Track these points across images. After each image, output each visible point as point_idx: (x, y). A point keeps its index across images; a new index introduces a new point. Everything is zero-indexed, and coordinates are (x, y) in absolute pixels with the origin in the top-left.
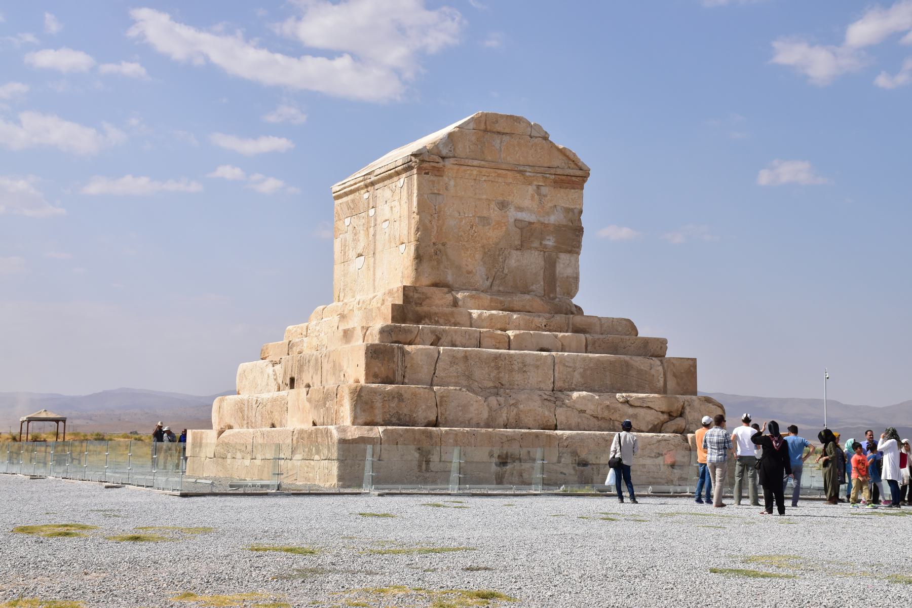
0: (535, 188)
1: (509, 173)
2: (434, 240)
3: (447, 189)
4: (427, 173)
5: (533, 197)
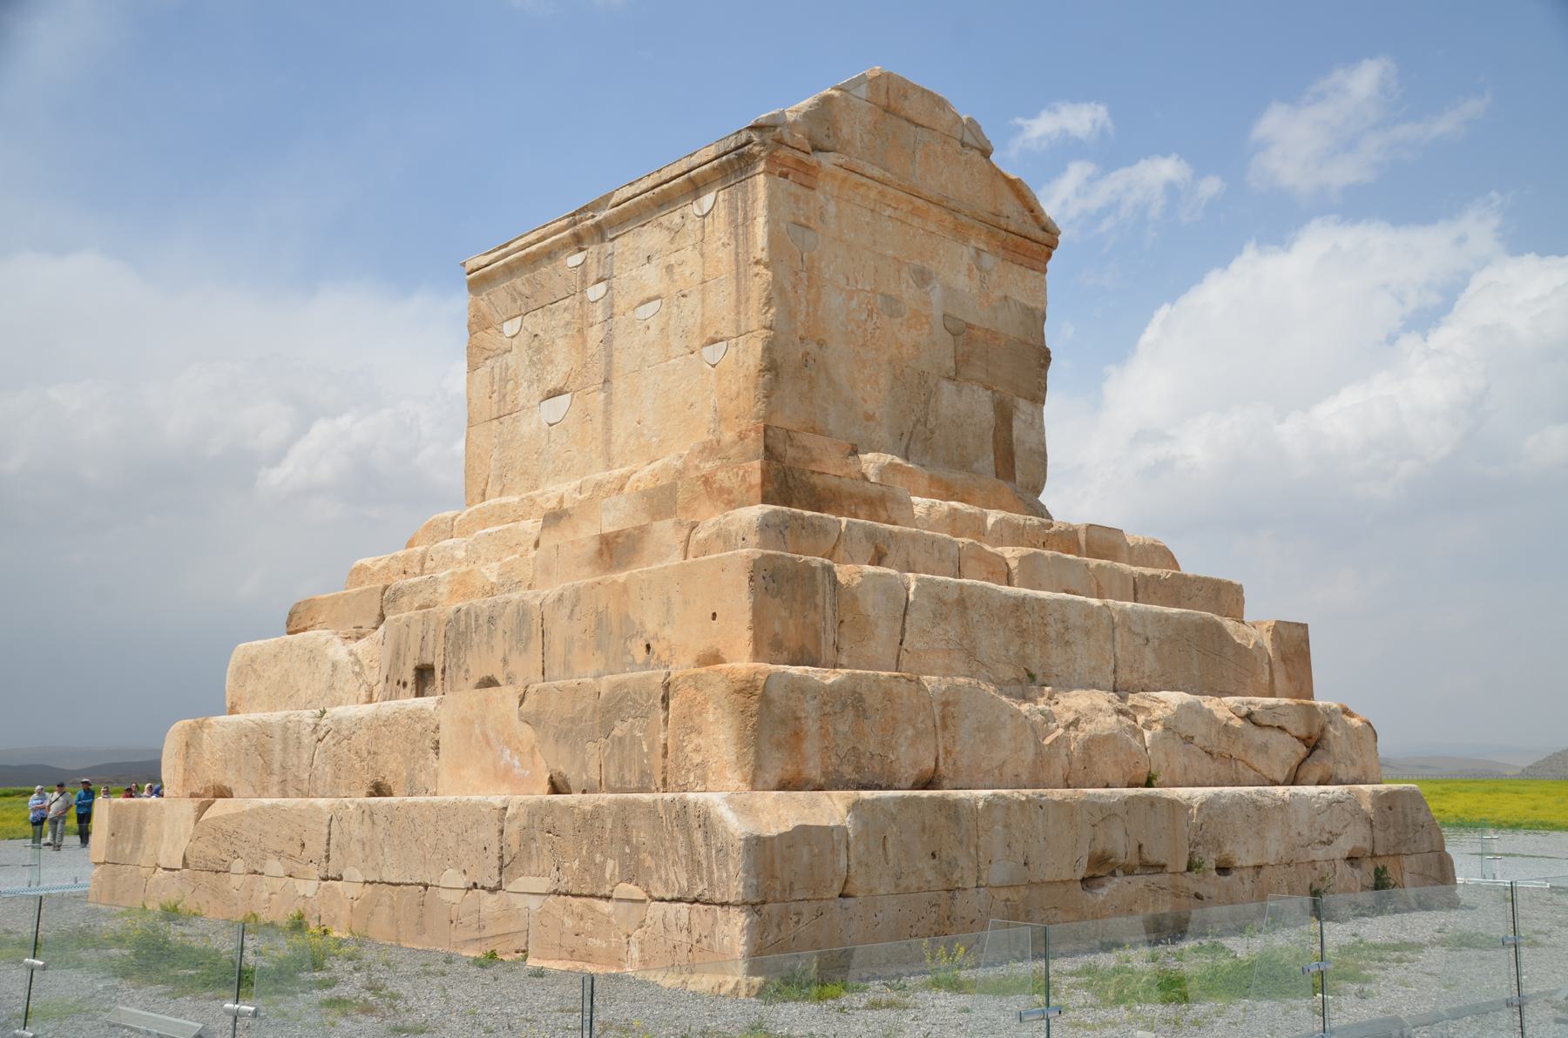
0: (973, 252)
1: (935, 210)
2: (801, 332)
3: (822, 218)
4: (785, 175)
5: (970, 270)
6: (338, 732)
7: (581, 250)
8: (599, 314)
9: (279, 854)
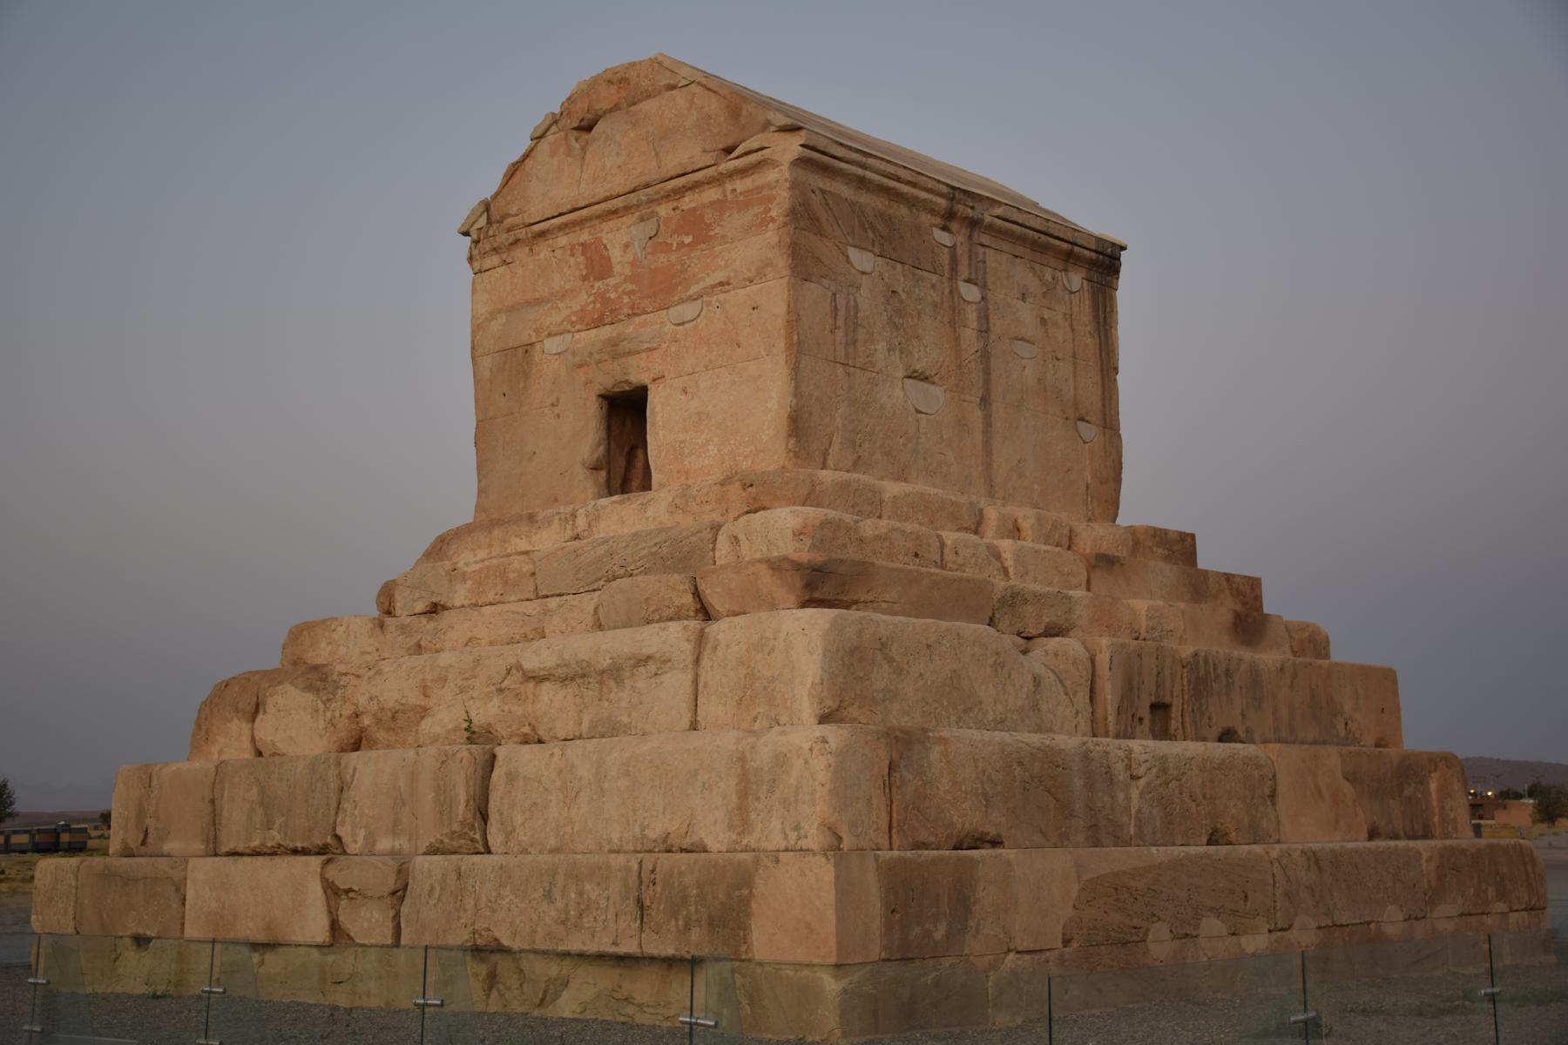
6: (1164, 770)
7: (945, 228)
8: (972, 315)
9: (1216, 911)
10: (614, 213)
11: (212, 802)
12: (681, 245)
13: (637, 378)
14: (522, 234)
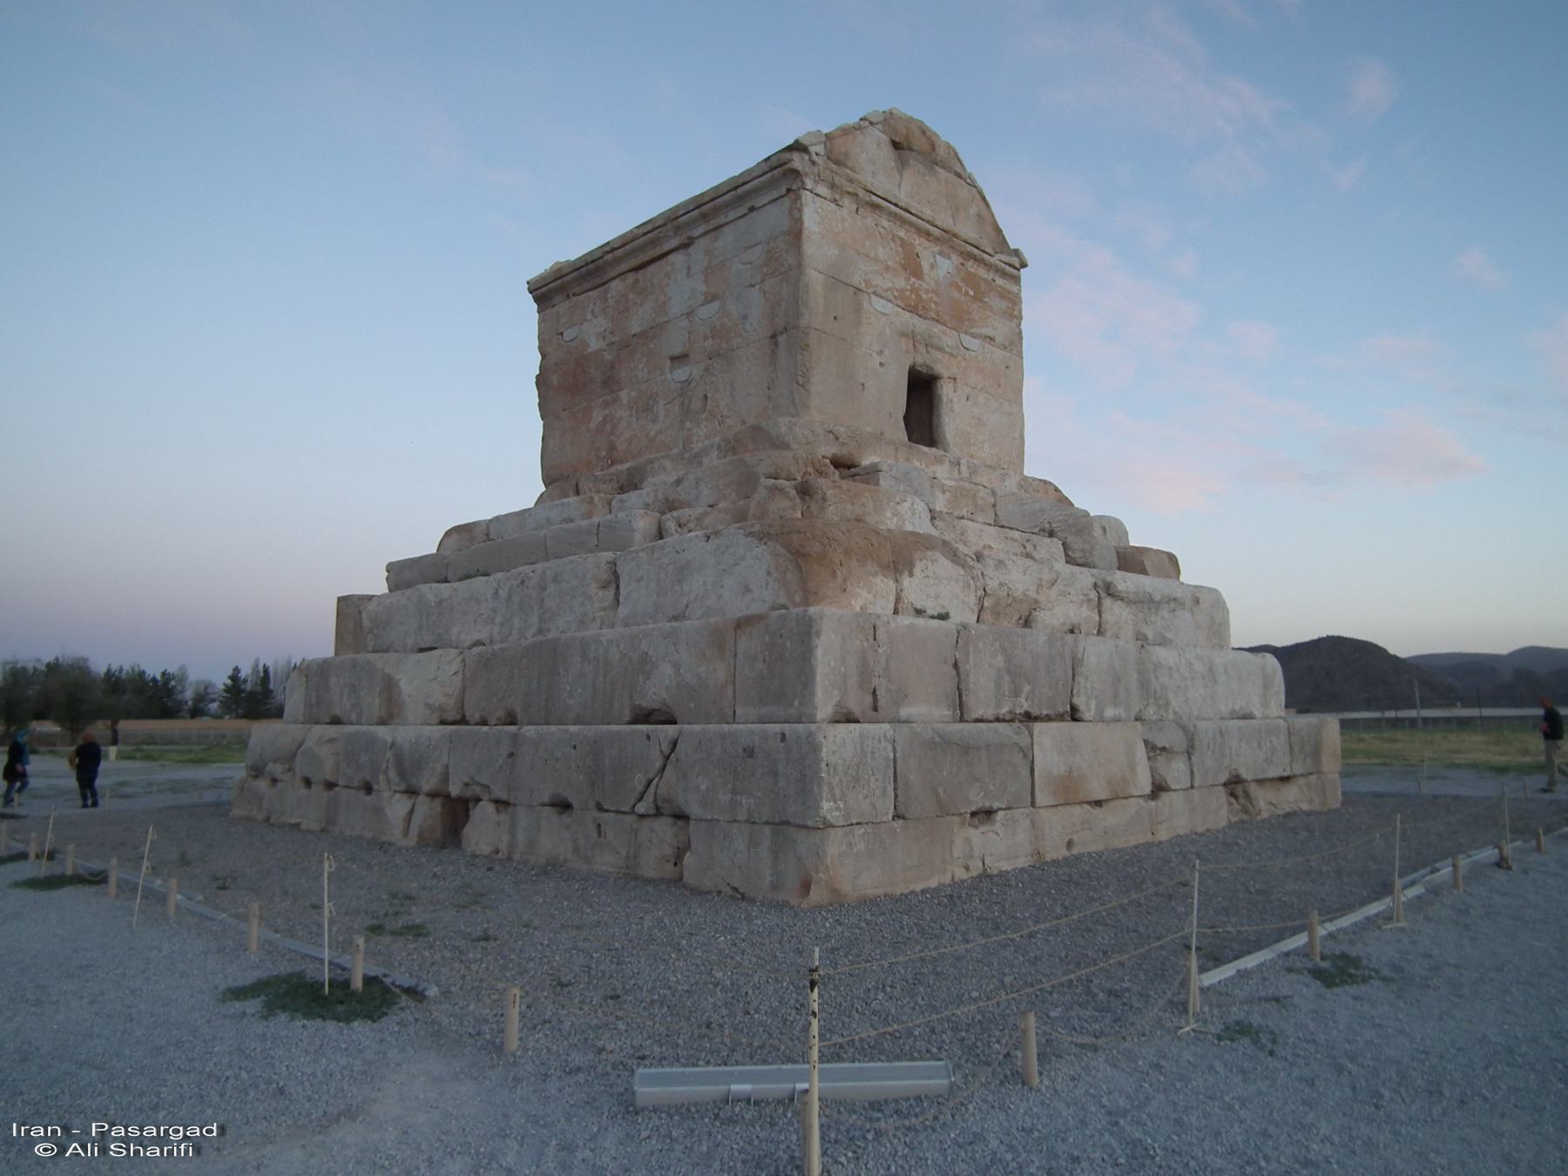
10: (928, 234)
11: (956, 665)
12: (967, 293)
13: (940, 369)
14: (861, 193)
